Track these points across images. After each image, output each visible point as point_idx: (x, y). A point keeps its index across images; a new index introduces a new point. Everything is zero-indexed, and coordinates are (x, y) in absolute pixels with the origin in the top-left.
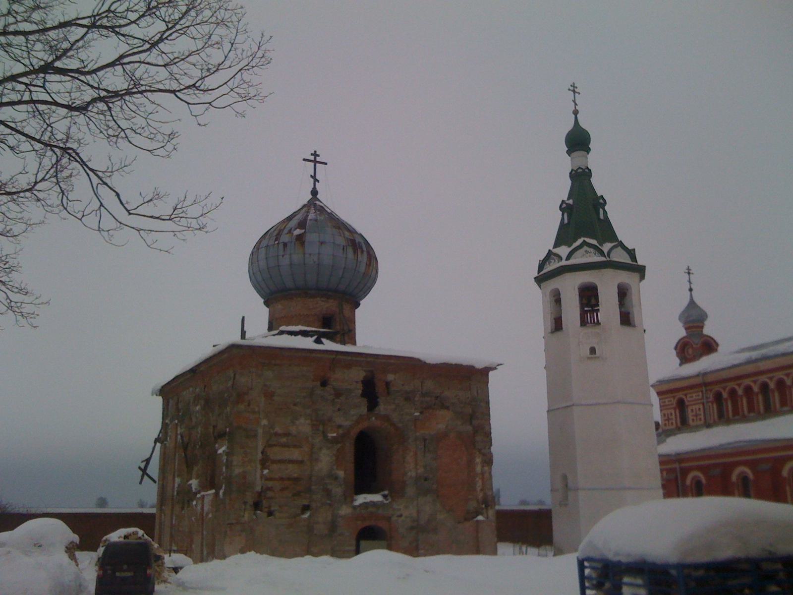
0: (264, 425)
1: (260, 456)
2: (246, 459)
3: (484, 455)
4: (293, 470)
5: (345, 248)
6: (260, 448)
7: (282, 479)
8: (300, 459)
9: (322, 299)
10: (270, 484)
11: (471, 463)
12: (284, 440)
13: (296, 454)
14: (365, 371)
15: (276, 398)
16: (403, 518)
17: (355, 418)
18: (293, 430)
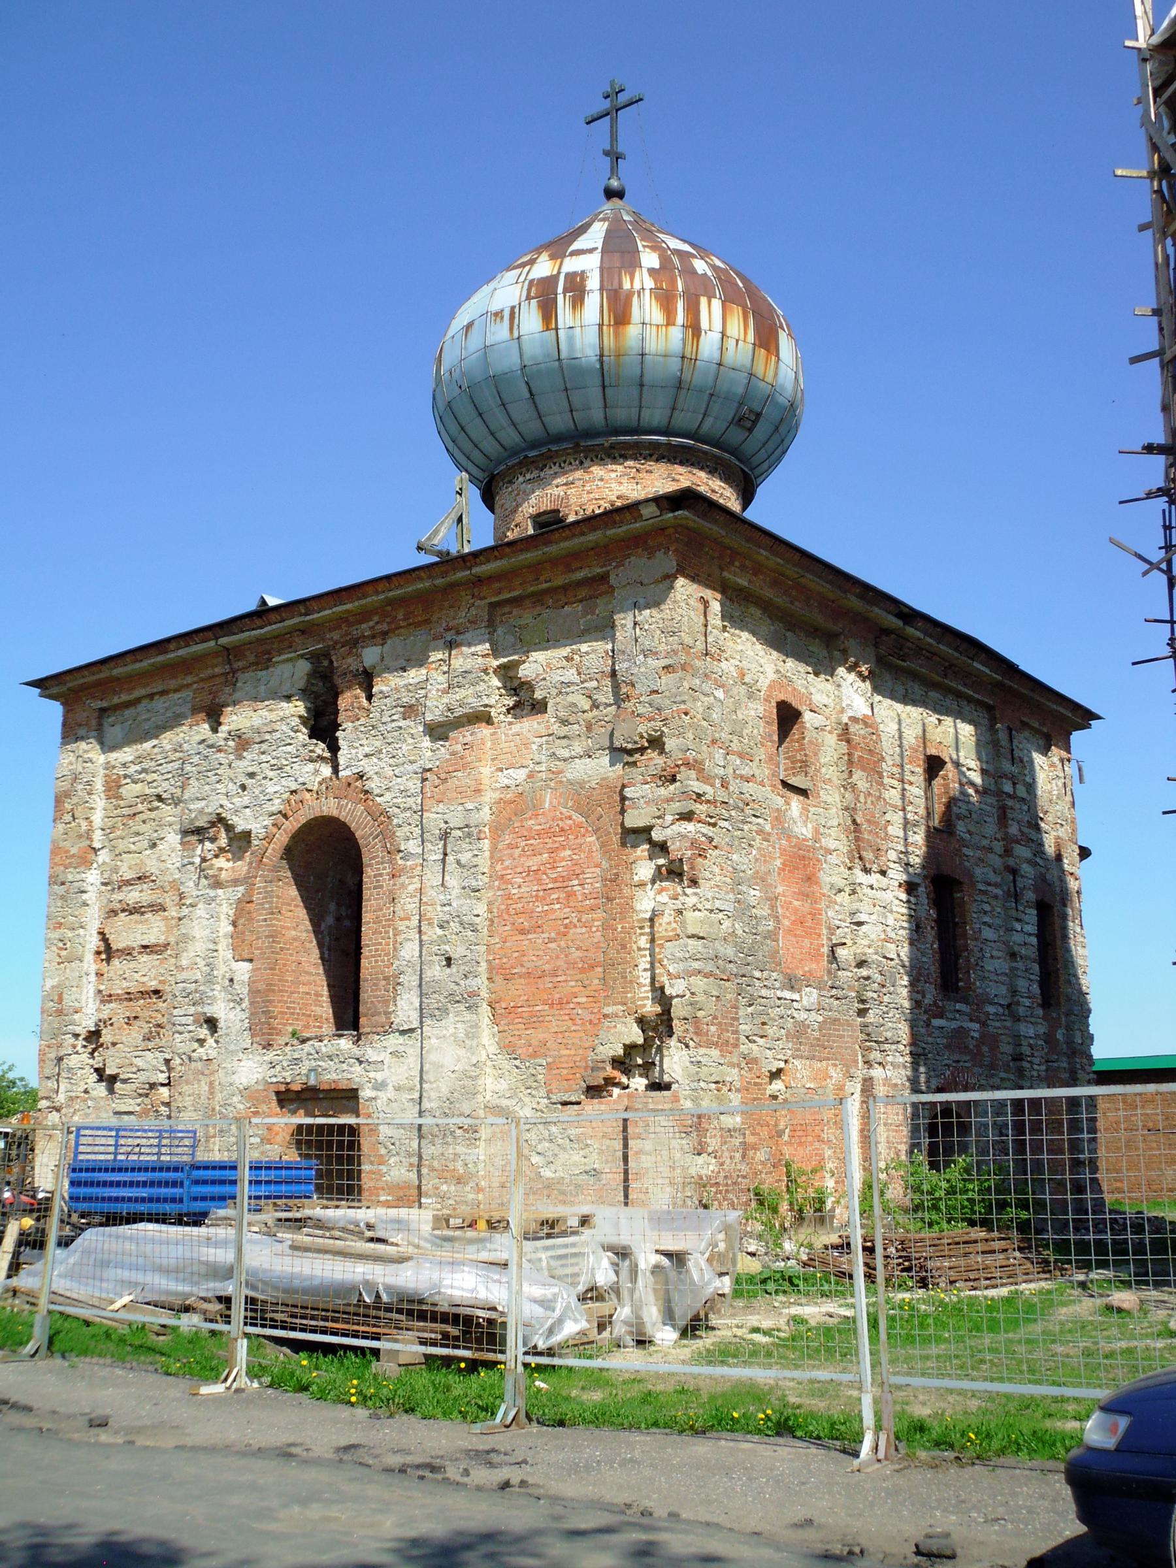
0: (104, 863)
1: (94, 942)
2: (64, 953)
3: (662, 848)
4: (145, 972)
5: (517, 310)
6: (94, 926)
7: (129, 997)
8: (162, 940)
9: (528, 476)
10: (106, 1011)
11: (615, 885)
12: (133, 896)
13: (152, 930)
14: (314, 658)
15: (123, 791)
16: (390, 1093)
17: (277, 805)
18: (152, 866)
